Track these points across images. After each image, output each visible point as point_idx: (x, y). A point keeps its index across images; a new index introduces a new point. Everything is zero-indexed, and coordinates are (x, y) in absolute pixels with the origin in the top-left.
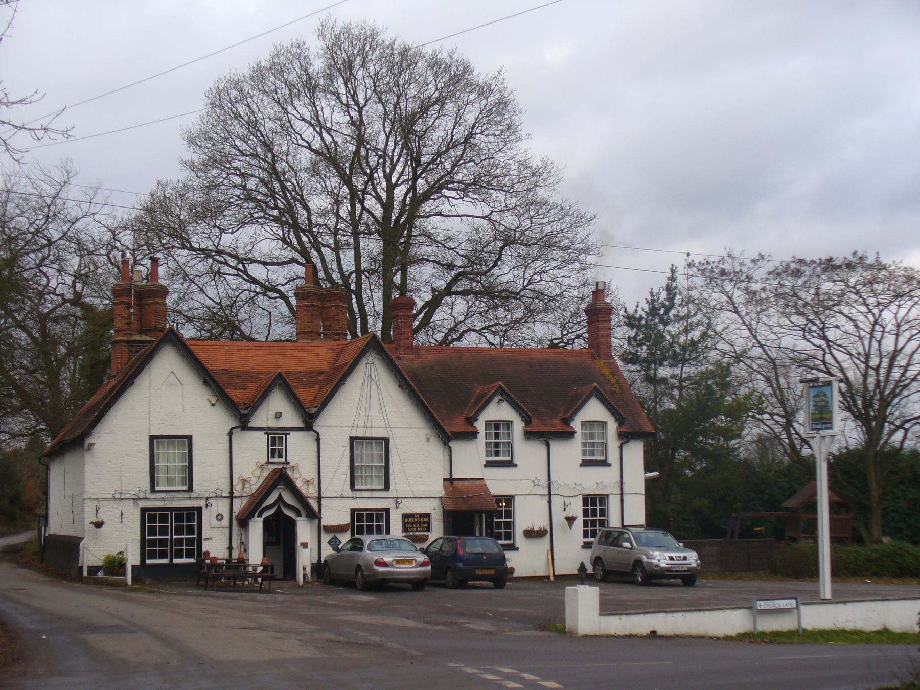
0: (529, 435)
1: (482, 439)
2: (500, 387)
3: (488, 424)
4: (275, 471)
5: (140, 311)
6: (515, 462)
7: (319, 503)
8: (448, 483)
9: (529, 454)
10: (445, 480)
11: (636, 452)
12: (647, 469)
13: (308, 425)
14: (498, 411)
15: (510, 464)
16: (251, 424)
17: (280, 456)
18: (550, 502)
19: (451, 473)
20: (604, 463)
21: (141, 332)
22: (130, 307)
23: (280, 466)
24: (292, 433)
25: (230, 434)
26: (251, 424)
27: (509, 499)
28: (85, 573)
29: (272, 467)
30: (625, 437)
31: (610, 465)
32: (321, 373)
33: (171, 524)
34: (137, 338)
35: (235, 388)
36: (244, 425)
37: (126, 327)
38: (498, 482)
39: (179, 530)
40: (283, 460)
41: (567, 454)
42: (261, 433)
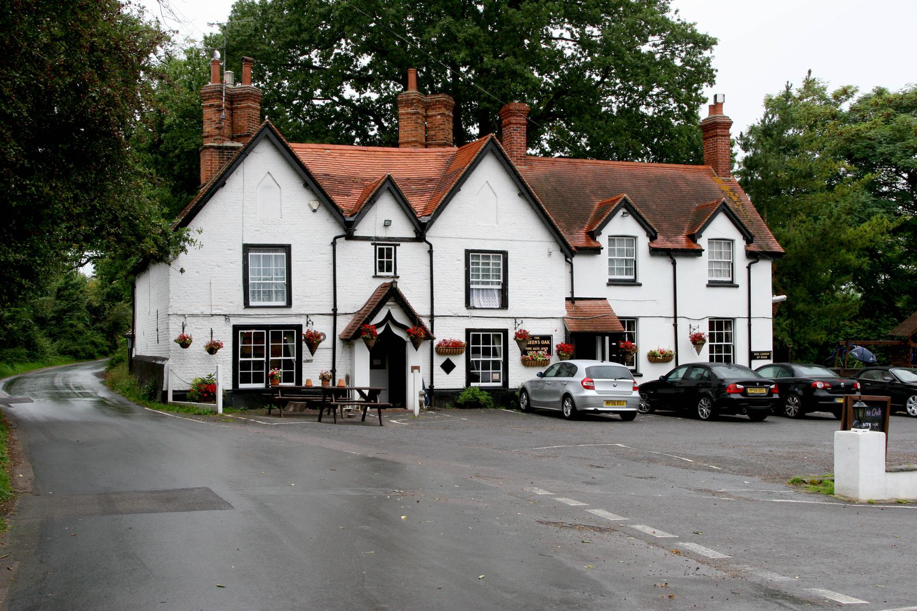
0: (655, 252)
1: (605, 252)
2: (625, 199)
3: (612, 239)
4: (384, 286)
5: (232, 116)
6: (639, 281)
7: (432, 322)
8: (569, 303)
9: (653, 271)
10: (567, 299)
11: (764, 271)
12: (776, 291)
13: (420, 234)
14: (622, 225)
15: (633, 283)
16: (356, 234)
17: (389, 270)
18: (675, 326)
19: (572, 292)
20: (731, 284)
21: (232, 139)
22: (220, 111)
23: (389, 281)
24: (402, 244)
25: (334, 244)
26: (356, 234)
27: (631, 323)
28: (170, 399)
29: (381, 282)
30: (753, 256)
31: (737, 286)
32: (430, 180)
33: (268, 344)
34: (229, 144)
35: (338, 195)
36: (349, 234)
37: (217, 131)
38: (622, 304)
39: (276, 352)
40: (392, 274)
41: (695, 272)
42: (369, 243)
